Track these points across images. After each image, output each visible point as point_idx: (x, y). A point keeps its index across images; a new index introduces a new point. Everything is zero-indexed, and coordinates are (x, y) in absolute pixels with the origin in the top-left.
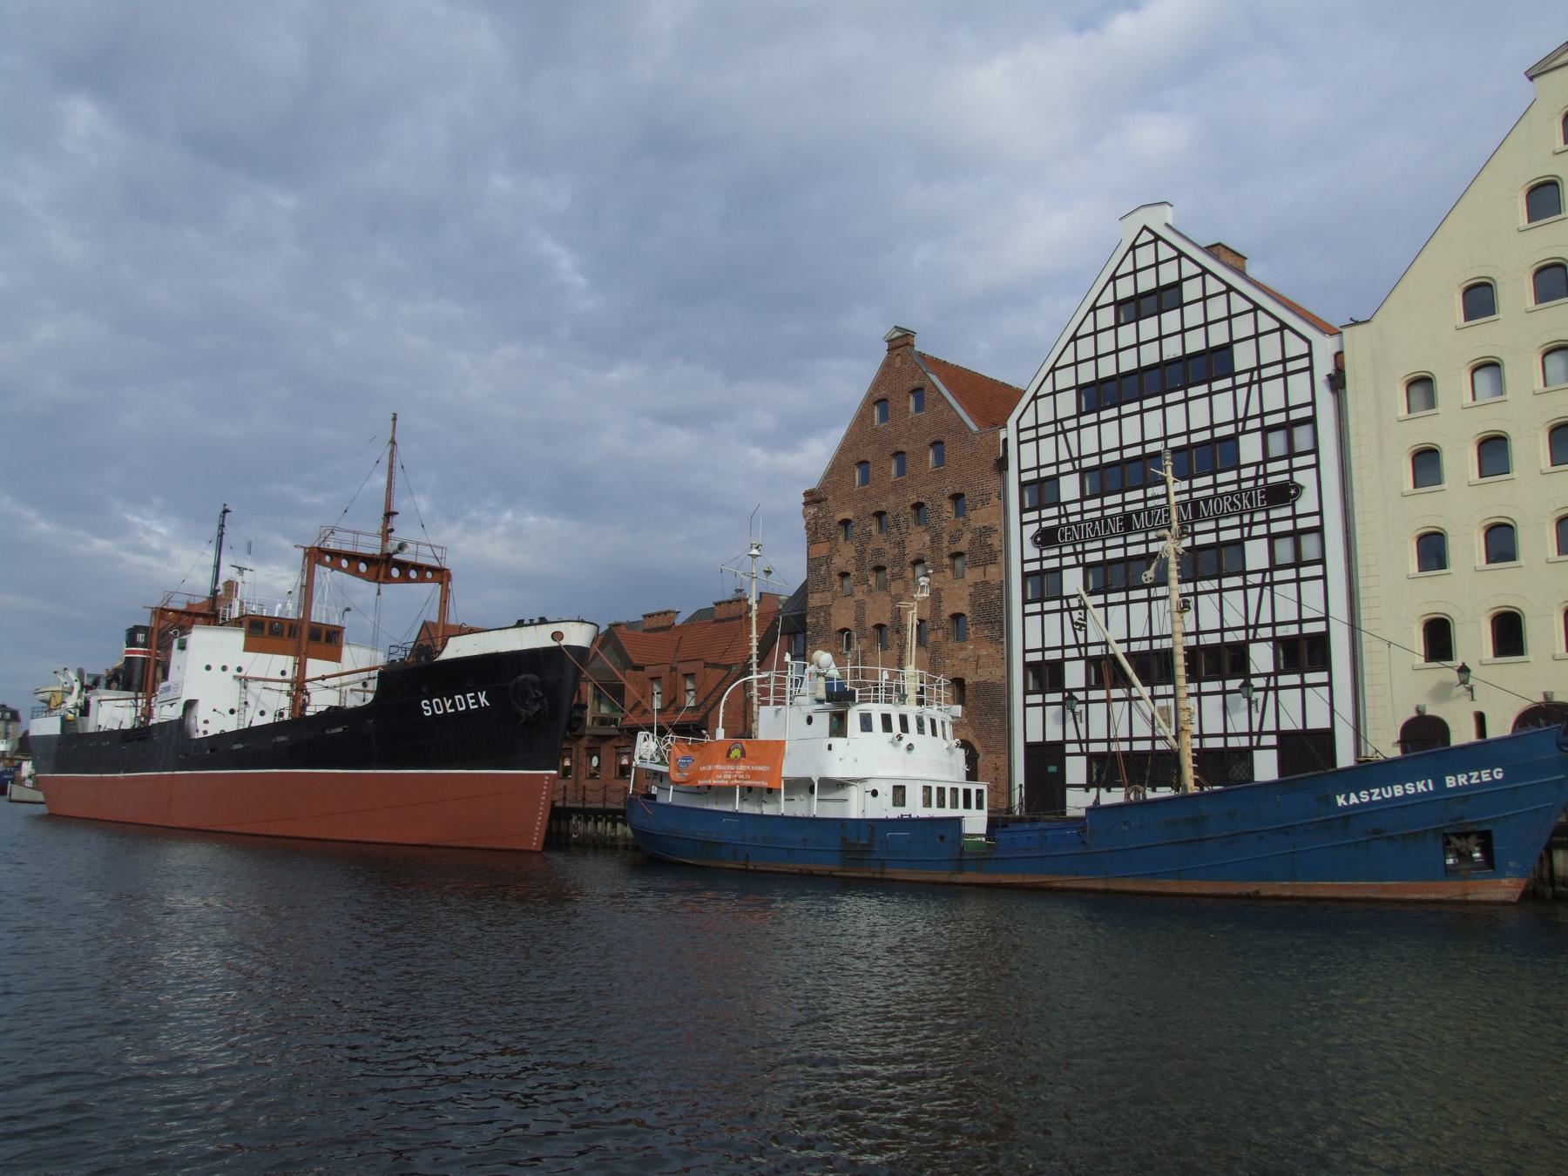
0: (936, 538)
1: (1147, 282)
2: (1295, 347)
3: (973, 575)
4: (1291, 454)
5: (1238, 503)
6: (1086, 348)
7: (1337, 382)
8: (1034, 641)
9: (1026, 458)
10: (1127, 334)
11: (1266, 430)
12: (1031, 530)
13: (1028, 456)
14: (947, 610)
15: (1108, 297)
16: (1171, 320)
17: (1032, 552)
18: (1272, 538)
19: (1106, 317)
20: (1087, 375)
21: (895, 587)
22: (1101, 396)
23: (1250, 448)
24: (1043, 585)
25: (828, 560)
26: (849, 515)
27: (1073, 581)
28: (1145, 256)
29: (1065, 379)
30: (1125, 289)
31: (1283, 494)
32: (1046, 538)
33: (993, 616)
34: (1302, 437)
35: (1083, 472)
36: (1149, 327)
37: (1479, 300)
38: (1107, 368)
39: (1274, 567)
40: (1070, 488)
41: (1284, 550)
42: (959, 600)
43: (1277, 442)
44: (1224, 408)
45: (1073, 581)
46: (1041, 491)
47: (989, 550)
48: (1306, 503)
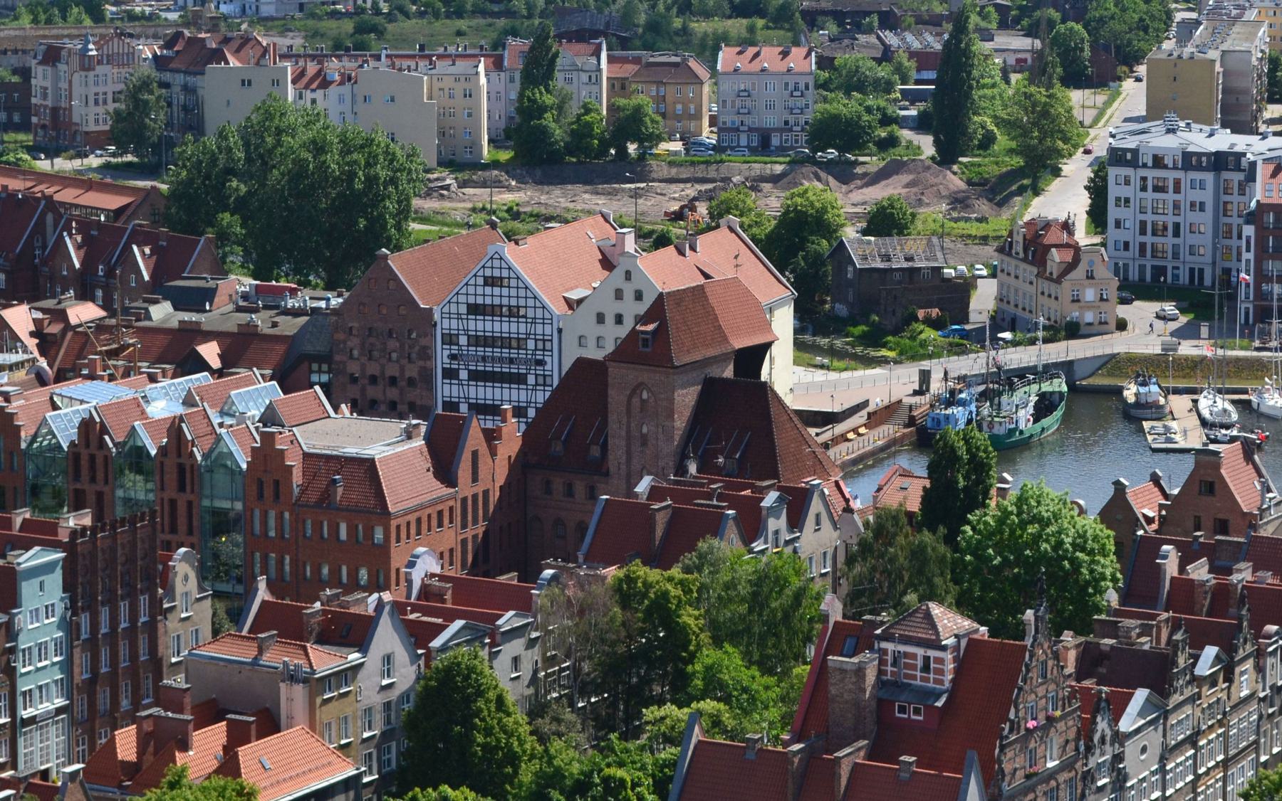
0: (402, 346)
1: (497, 273)
2: (547, 315)
3: (421, 363)
4: (544, 350)
5: (526, 362)
6: (471, 290)
7: (560, 331)
8: (447, 393)
9: (444, 325)
10: (488, 290)
11: (536, 340)
12: (446, 353)
13: (446, 325)
14: (408, 374)
15: (481, 273)
16: (505, 291)
17: (446, 360)
18: (536, 375)
19: (480, 281)
20: (471, 300)
21: (384, 361)
22: (474, 309)
23: (531, 345)
24: (450, 374)
25: (345, 342)
26: (356, 325)
27: (464, 375)
28: (496, 263)
29: (462, 299)
30: (488, 273)
31: (541, 363)
32: (453, 357)
33: (427, 378)
34: (548, 345)
35: (469, 336)
36: (497, 290)
37: (600, 318)
38: (480, 300)
39: (537, 384)
40: (463, 340)
41: (541, 380)
42: (412, 371)
43: (540, 345)
44: (522, 328)
45: (464, 375)
46: (450, 339)
47: (427, 354)
48: (548, 367)
